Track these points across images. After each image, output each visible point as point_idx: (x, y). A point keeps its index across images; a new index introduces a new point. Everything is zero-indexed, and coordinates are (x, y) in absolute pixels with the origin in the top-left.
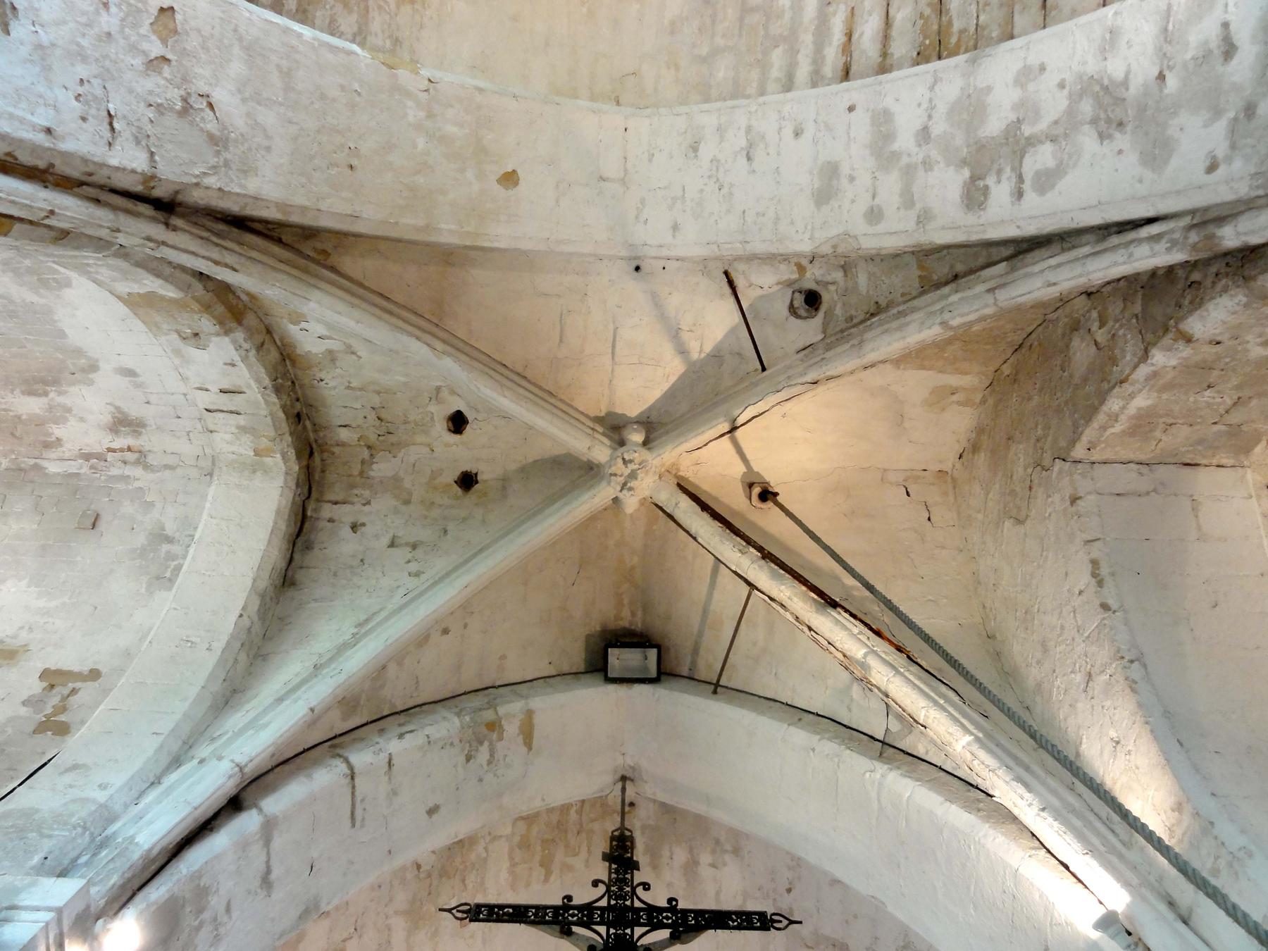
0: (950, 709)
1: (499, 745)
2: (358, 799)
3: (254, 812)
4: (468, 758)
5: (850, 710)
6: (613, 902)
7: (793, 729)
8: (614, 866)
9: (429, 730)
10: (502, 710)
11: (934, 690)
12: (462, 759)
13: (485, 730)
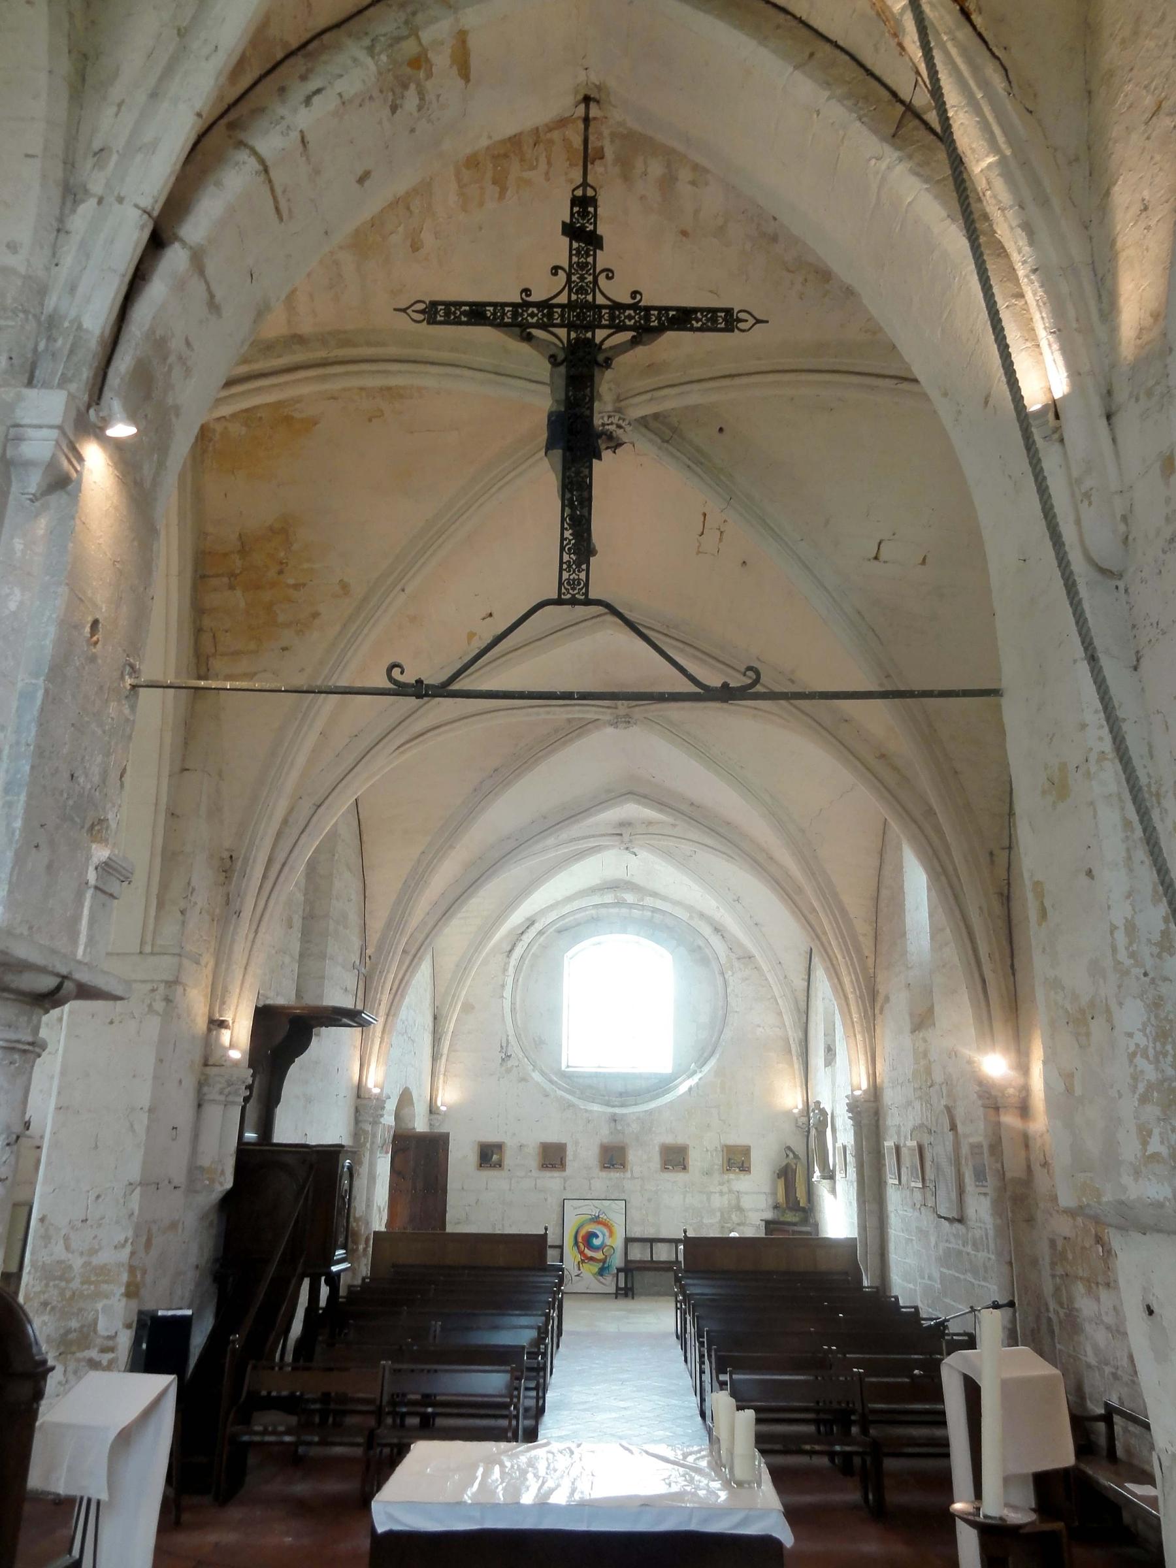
0: (987, 110)
1: (429, 85)
2: (279, 191)
3: (177, 246)
4: (394, 109)
5: (876, 50)
6: (574, 297)
7: (799, 76)
8: (575, 245)
9: (340, 86)
10: (426, 36)
11: (976, 70)
12: (387, 111)
13: (408, 70)
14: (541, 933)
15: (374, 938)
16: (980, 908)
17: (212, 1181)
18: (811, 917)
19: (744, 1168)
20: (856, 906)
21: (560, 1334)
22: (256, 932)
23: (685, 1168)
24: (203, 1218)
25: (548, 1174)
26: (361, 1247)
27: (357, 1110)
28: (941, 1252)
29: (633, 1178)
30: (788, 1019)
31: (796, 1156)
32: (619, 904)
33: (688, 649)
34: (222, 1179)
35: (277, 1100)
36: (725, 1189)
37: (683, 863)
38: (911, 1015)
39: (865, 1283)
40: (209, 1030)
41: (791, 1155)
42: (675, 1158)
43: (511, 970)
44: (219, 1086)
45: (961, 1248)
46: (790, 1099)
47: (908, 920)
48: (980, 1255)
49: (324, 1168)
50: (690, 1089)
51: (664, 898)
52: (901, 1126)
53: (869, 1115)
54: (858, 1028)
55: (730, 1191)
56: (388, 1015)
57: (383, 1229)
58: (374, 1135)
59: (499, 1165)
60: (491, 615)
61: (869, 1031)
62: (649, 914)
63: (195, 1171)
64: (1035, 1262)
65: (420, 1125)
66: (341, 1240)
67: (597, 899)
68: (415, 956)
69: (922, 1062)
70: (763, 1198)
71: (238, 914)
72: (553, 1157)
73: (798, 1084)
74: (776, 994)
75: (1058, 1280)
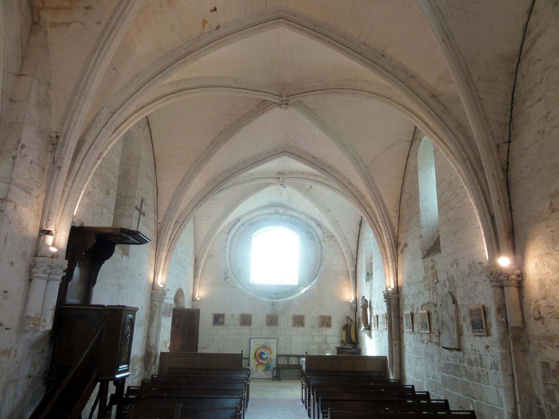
14: (242, 225)
15: (162, 214)
16: (493, 175)
17: (36, 325)
18: (368, 210)
19: (329, 325)
20: (390, 203)
21: (248, 400)
22: (73, 182)
23: (303, 325)
24: (34, 346)
25: (243, 327)
26: (152, 360)
27: (152, 295)
28: (442, 365)
29: (280, 329)
30: (348, 262)
31: (351, 320)
32: (277, 213)
33: (326, 38)
34: (44, 324)
35: (94, 283)
36: (320, 334)
37: (306, 192)
38: (423, 250)
39: (392, 377)
40: (40, 236)
41: (349, 320)
42: (299, 321)
43: (229, 241)
44: (43, 269)
45: (458, 363)
46: (349, 296)
47: (421, 205)
48: (474, 368)
49: (117, 320)
50: (306, 291)
51: (296, 211)
52: (412, 303)
53: (394, 300)
54: (389, 260)
55: (323, 335)
56: (168, 251)
57: (167, 351)
58: (160, 307)
59: (222, 323)
60: (215, 9)
61: (395, 262)
62: (289, 218)
63: (24, 319)
64: (528, 375)
65: (187, 305)
66: (124, 359)
67: (267, 211)
68: (182, 224)
69: (430, 272)
70: (336, 338)
71: (59, 168)
72: (246, 320)
73: (352, 288)
74: (344, 252)
75: (551, 387)
